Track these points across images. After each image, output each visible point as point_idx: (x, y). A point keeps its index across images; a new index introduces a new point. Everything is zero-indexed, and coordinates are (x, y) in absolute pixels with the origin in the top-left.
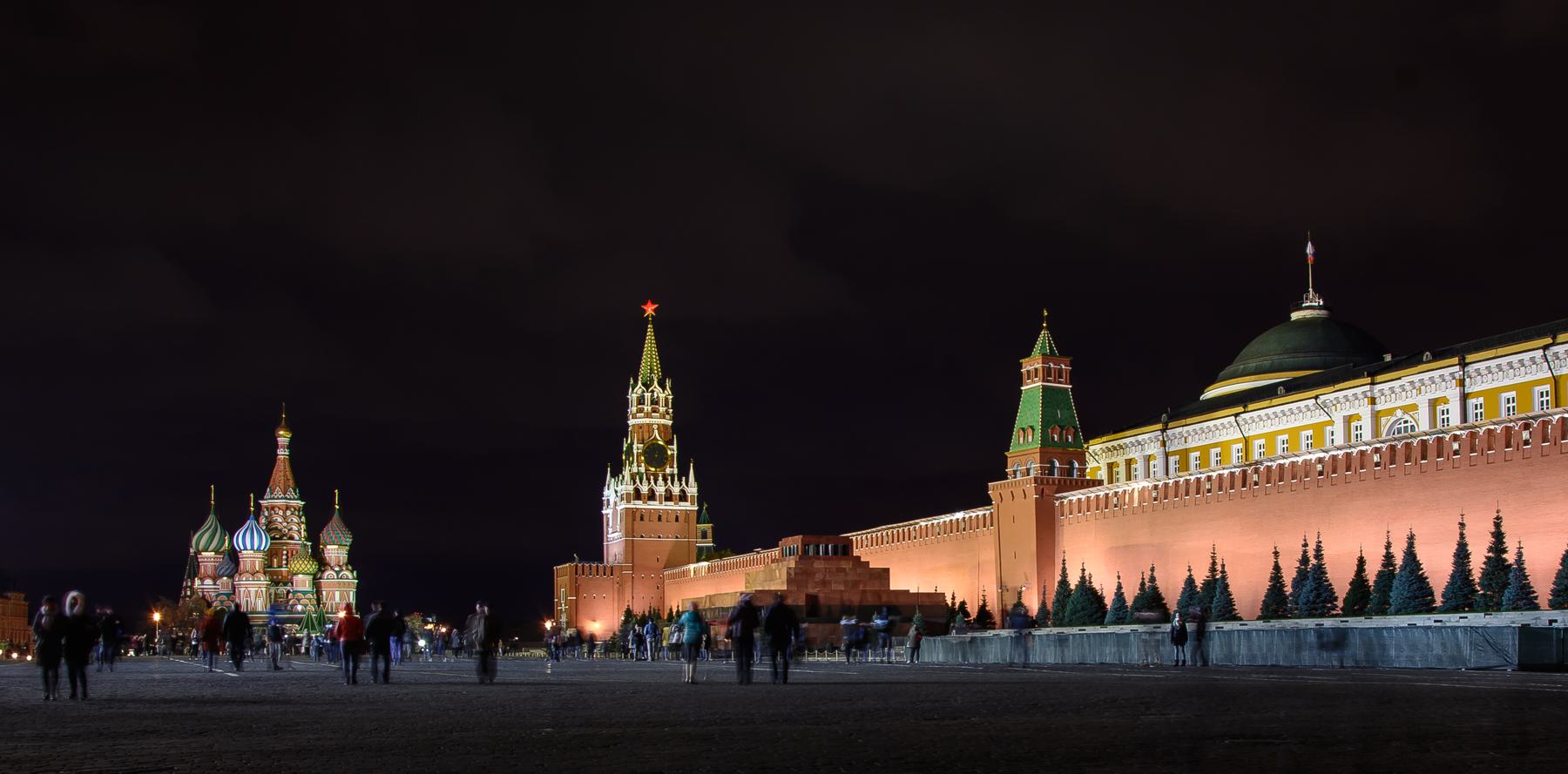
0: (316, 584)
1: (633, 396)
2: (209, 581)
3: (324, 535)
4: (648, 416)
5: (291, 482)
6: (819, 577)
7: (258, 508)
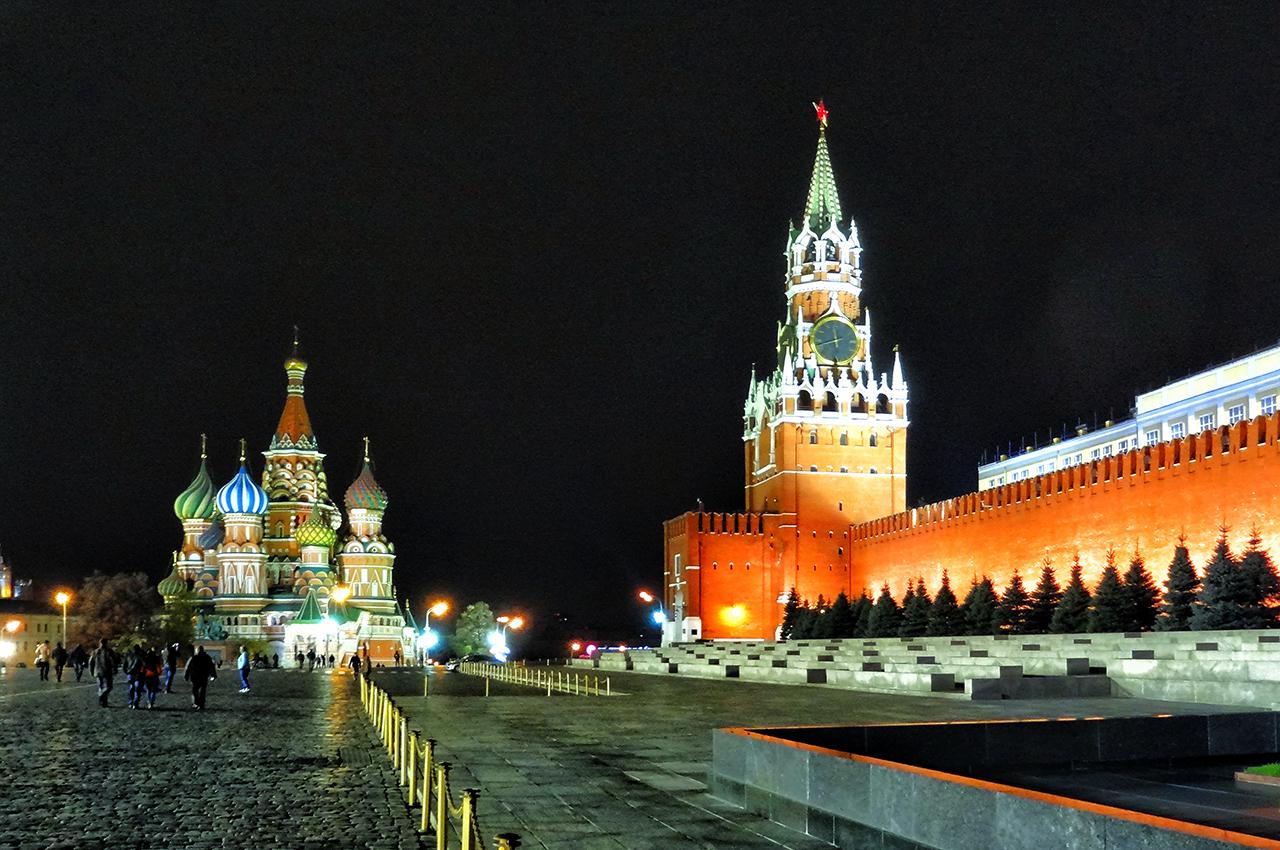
1: (797, 247)
2: (195, 556)
3: (351, 495)
5: (307, 427)
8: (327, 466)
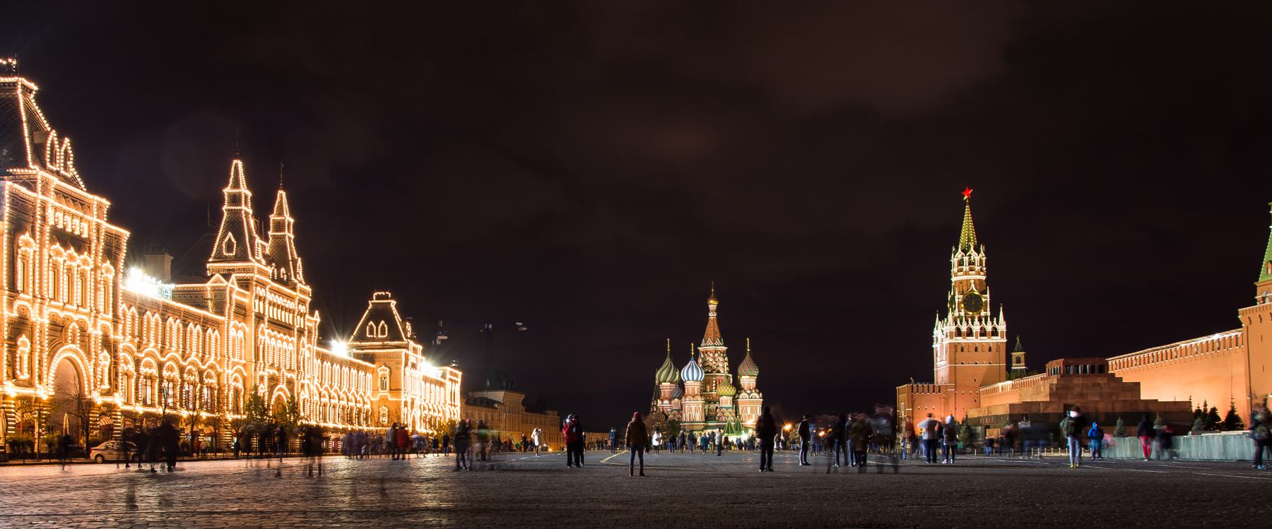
0: (735, 401)
1: (954, 260)
2: (666, 402)
3: (741, 369)
4: (966, 274)
6: (1077, 390)
7: (697, 352)
8: (728, 353)
